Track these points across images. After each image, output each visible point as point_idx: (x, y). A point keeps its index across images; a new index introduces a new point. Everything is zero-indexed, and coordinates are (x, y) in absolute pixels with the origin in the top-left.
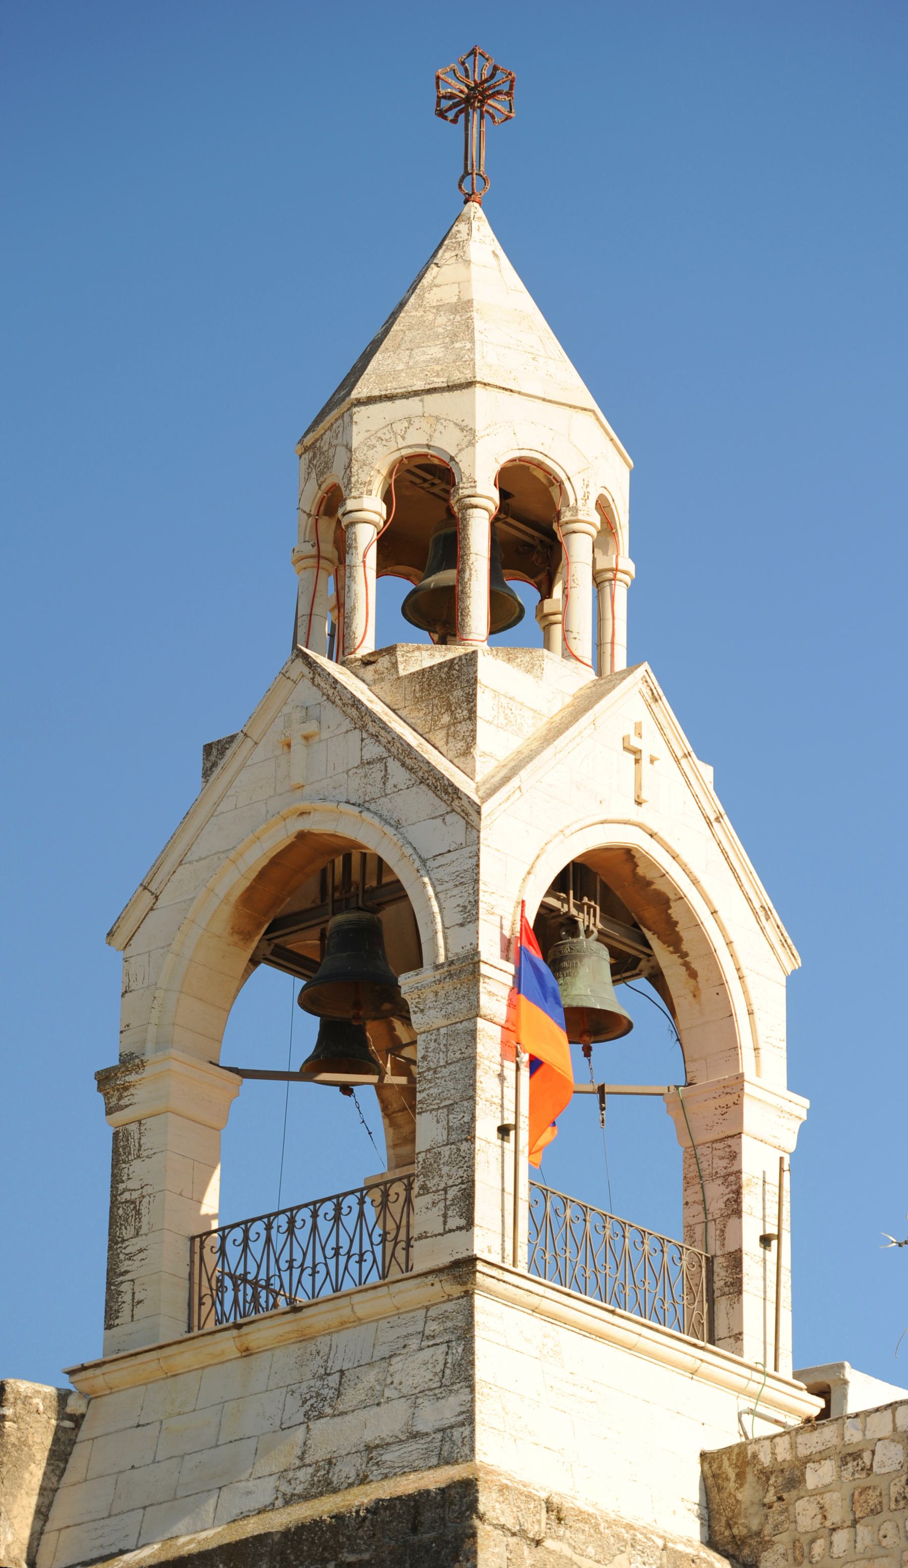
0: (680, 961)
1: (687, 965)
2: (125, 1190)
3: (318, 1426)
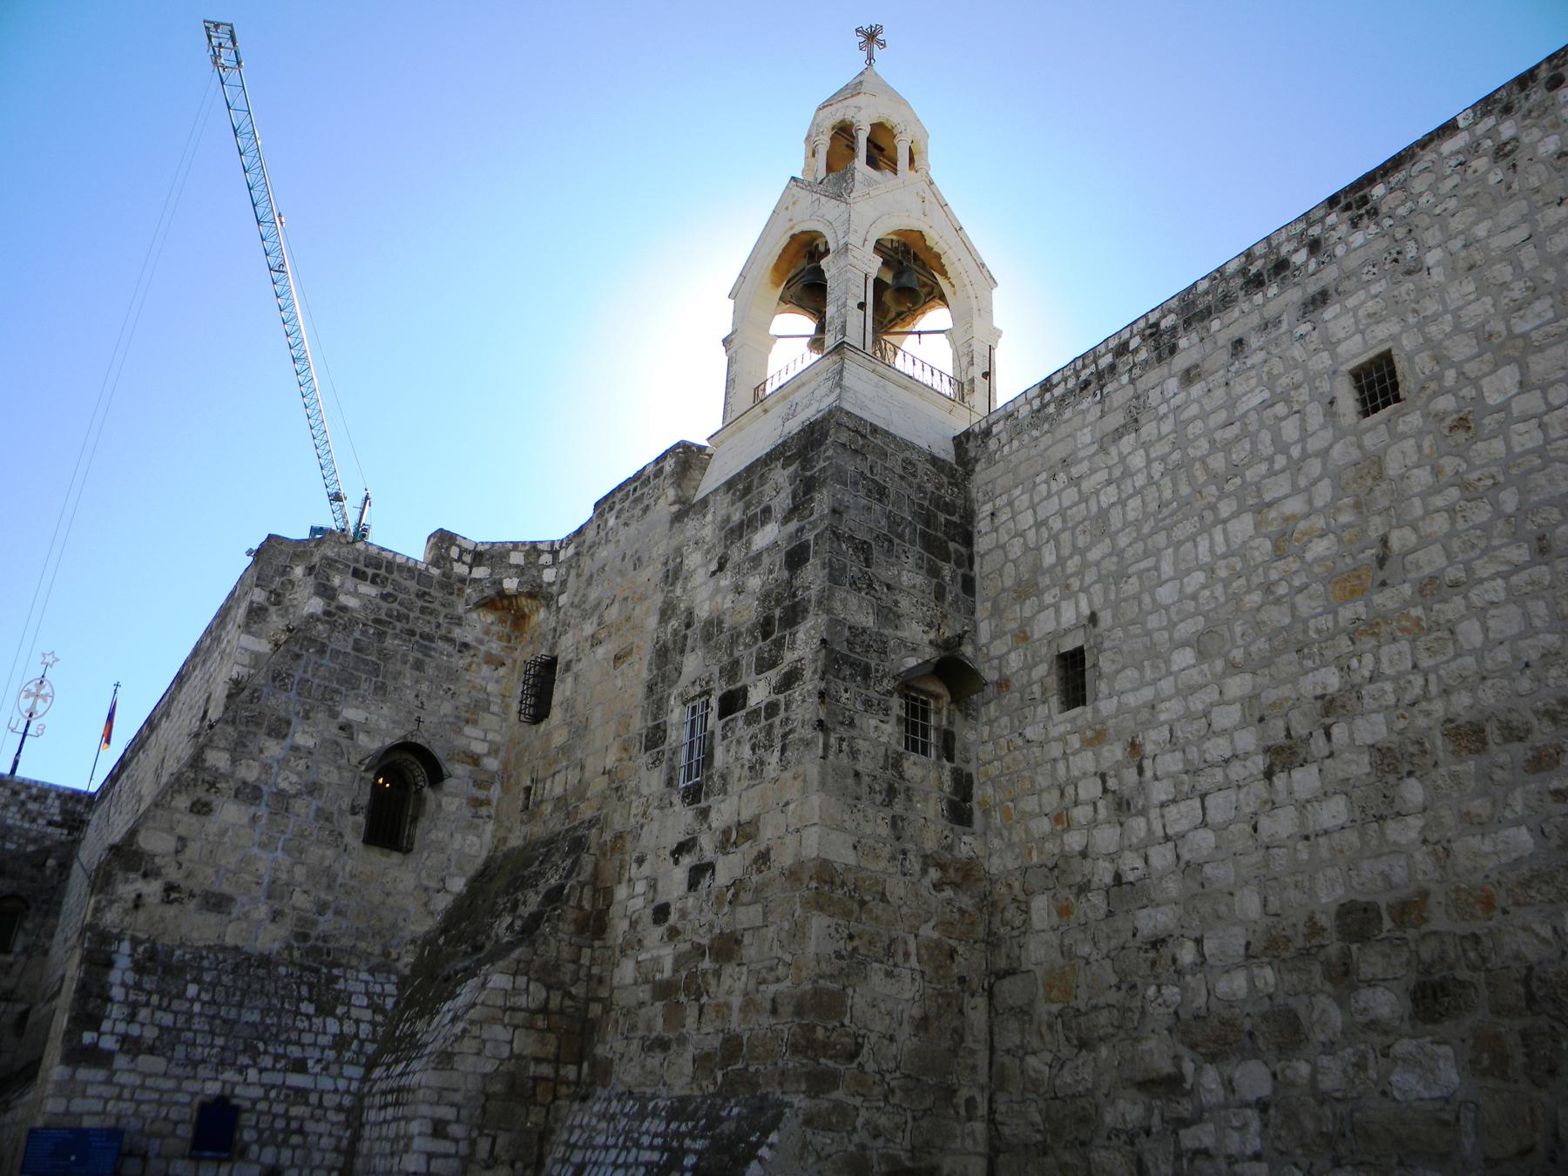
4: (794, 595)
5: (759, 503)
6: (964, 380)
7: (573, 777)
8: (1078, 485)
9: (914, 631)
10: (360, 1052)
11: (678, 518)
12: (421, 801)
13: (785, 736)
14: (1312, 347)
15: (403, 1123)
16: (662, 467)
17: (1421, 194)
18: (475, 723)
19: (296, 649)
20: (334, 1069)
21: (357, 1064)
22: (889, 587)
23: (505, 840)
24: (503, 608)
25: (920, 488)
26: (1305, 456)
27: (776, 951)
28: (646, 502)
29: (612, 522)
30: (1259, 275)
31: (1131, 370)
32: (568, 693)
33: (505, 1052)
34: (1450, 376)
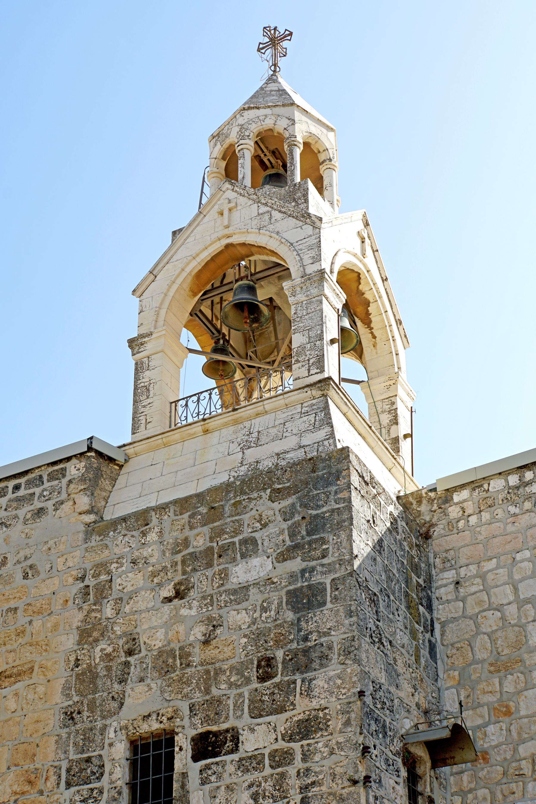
0: (370, 331)
1: (372, 333)
2: (141, 383)
3: (248, 452)
4: (306, 639)
5: (236, 532)
16: (64, 470)
28: (37, 504)
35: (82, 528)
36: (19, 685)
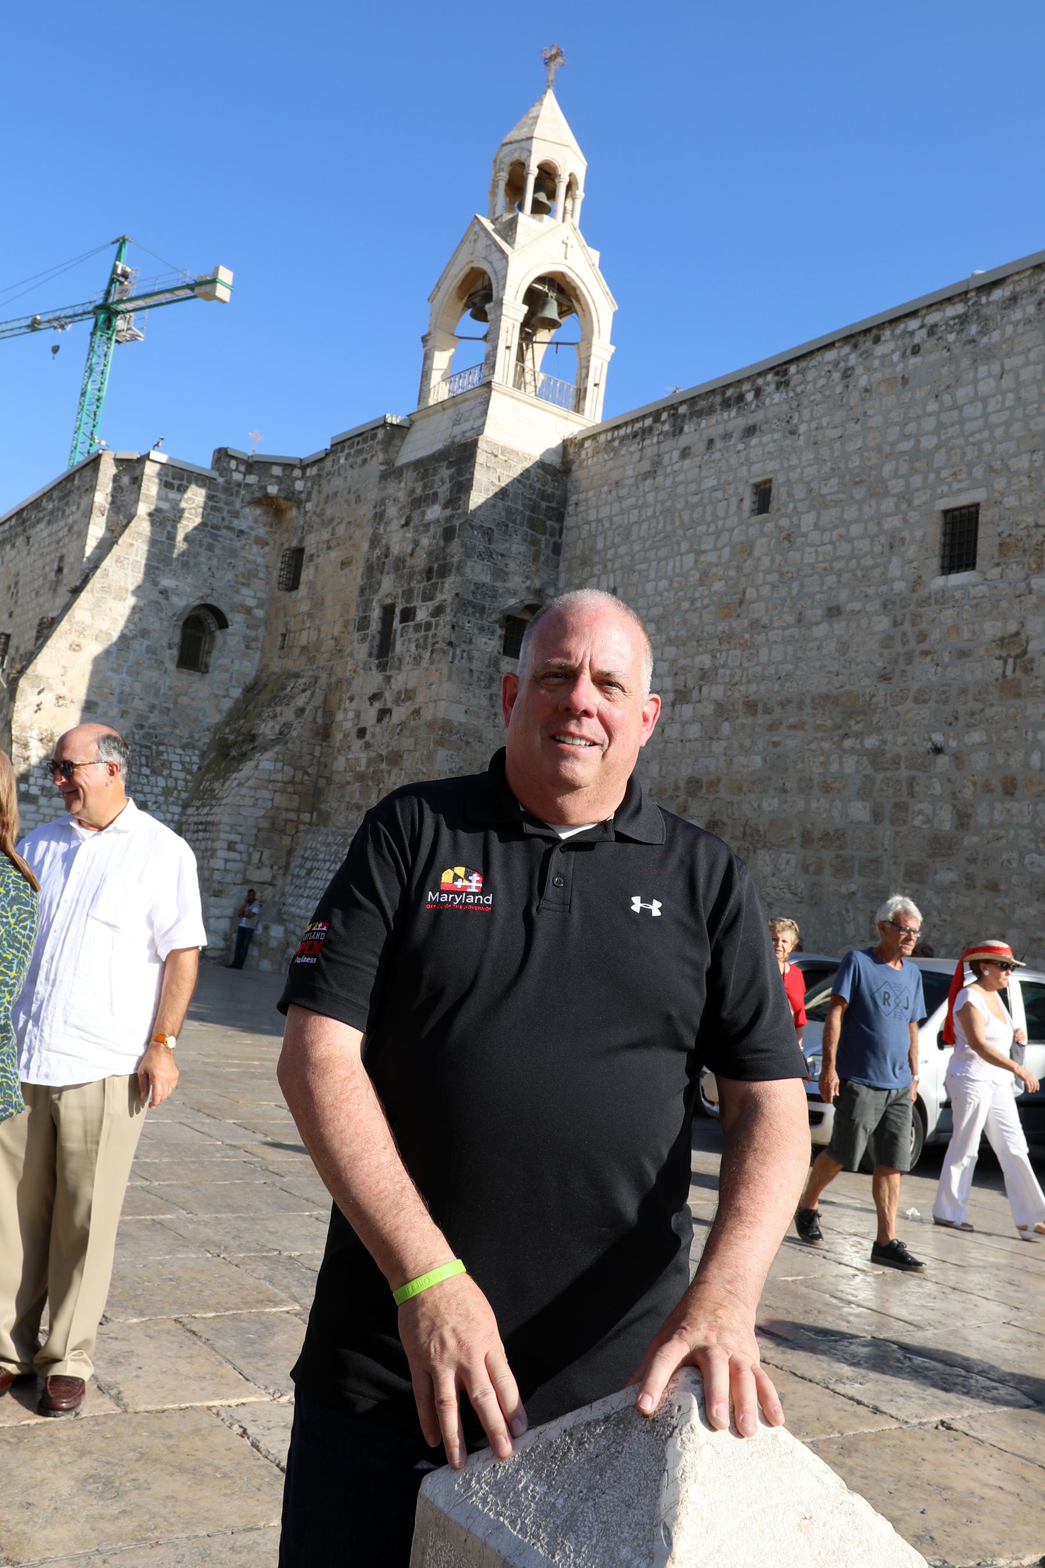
4: (445, 559)
5: (432, 487)
6: (582, 387)
7: (314, 637)
8: (620, 502)
9: (516, 582)
10: (178, 798)
11: (384, 476)
12: (213, 639)
13: (434, 644)
14: (741, 461)
15: (209, 842)
17: (809, 383)
18: (248, 585)
19: (130, 541)
20: (164, 807)
21: (177, 805)
22: (502, 555)
23: (267, 666)
24: (267, 504)
25: (531, 487)
26: (723, 530)
27: (420, 766)
28: (365, 456)
29: (342, 461)
30: (729, 398)
31: (659, 435)
32: (311, 577)
33: (269, 804)
34: (791, 506)
35: (378, 474)
36: (347, 570)
